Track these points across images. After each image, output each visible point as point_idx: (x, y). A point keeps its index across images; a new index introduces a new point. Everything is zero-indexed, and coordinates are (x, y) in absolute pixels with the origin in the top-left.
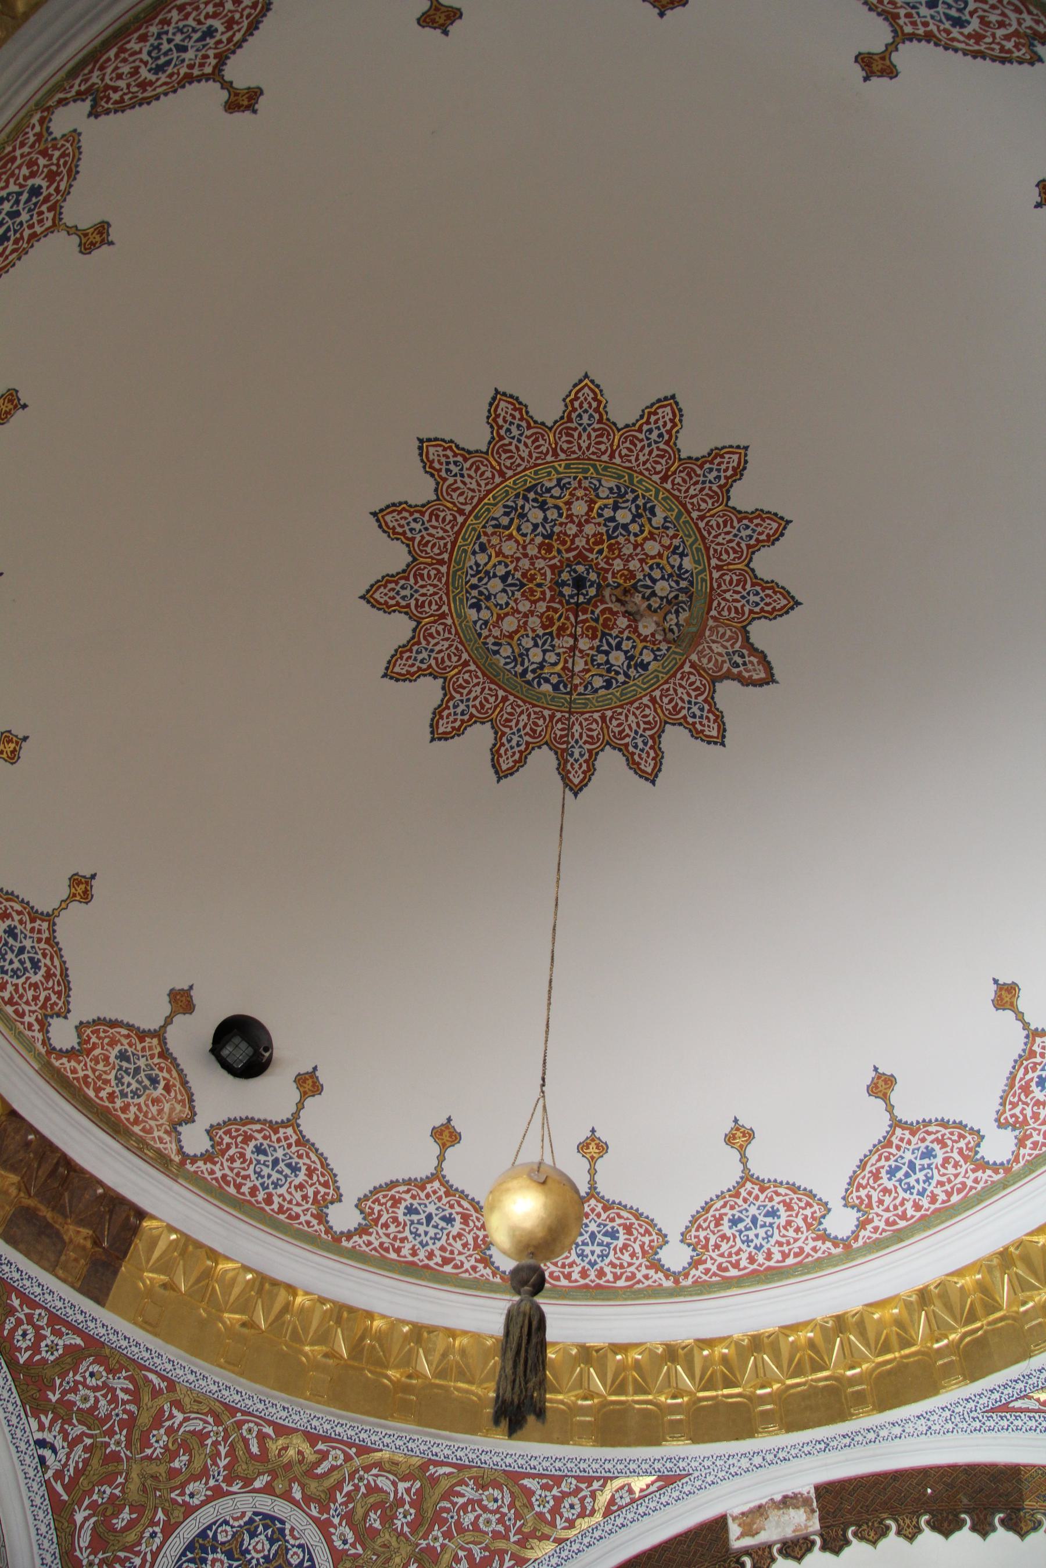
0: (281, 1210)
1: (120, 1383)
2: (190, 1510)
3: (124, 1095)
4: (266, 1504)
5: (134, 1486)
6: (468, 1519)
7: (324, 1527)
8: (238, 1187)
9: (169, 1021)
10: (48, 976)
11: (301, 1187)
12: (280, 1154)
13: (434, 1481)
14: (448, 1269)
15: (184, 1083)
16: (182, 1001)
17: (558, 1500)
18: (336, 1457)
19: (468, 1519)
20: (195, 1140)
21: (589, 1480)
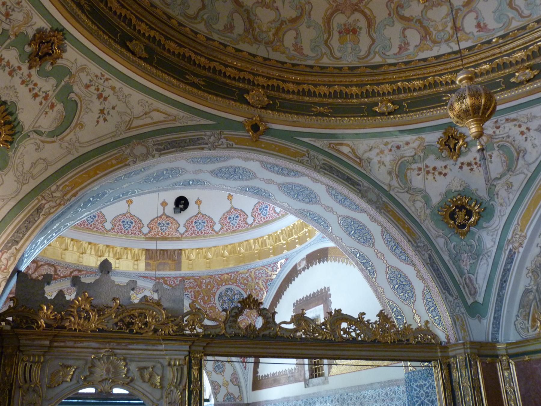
0: (205, 233)
1: (192, 281)
2: (215, 293)
3: (164, 231)
4: (227, 287)
5: (204, 293)
6: (260, 276)
7: (238, 286)
8: (195, 234)
9: (164, 210)
10: (135, 222)
11: (207, 225)
12: (200, 221)
13: (251, 272)
14: (240, 228)
15: (174, 220)
16: (164, 204)
17: (272, 268)
18: (233, 275)
19: (260, 276)
20: (182, 230)
21: (275, 263)
